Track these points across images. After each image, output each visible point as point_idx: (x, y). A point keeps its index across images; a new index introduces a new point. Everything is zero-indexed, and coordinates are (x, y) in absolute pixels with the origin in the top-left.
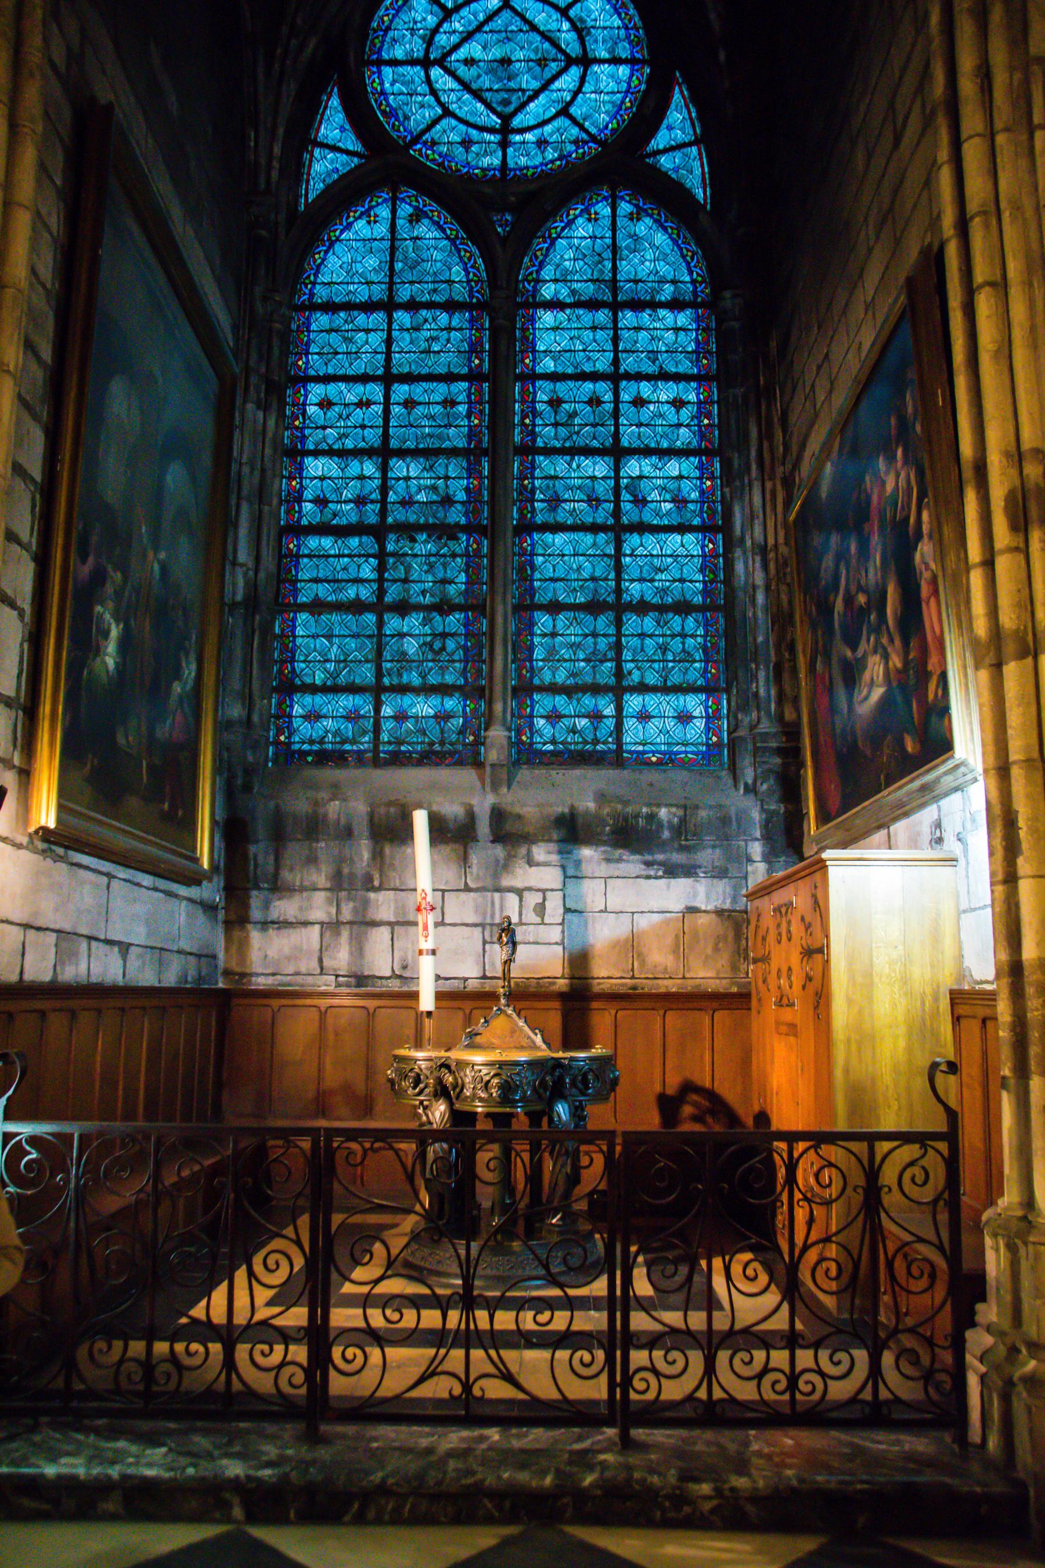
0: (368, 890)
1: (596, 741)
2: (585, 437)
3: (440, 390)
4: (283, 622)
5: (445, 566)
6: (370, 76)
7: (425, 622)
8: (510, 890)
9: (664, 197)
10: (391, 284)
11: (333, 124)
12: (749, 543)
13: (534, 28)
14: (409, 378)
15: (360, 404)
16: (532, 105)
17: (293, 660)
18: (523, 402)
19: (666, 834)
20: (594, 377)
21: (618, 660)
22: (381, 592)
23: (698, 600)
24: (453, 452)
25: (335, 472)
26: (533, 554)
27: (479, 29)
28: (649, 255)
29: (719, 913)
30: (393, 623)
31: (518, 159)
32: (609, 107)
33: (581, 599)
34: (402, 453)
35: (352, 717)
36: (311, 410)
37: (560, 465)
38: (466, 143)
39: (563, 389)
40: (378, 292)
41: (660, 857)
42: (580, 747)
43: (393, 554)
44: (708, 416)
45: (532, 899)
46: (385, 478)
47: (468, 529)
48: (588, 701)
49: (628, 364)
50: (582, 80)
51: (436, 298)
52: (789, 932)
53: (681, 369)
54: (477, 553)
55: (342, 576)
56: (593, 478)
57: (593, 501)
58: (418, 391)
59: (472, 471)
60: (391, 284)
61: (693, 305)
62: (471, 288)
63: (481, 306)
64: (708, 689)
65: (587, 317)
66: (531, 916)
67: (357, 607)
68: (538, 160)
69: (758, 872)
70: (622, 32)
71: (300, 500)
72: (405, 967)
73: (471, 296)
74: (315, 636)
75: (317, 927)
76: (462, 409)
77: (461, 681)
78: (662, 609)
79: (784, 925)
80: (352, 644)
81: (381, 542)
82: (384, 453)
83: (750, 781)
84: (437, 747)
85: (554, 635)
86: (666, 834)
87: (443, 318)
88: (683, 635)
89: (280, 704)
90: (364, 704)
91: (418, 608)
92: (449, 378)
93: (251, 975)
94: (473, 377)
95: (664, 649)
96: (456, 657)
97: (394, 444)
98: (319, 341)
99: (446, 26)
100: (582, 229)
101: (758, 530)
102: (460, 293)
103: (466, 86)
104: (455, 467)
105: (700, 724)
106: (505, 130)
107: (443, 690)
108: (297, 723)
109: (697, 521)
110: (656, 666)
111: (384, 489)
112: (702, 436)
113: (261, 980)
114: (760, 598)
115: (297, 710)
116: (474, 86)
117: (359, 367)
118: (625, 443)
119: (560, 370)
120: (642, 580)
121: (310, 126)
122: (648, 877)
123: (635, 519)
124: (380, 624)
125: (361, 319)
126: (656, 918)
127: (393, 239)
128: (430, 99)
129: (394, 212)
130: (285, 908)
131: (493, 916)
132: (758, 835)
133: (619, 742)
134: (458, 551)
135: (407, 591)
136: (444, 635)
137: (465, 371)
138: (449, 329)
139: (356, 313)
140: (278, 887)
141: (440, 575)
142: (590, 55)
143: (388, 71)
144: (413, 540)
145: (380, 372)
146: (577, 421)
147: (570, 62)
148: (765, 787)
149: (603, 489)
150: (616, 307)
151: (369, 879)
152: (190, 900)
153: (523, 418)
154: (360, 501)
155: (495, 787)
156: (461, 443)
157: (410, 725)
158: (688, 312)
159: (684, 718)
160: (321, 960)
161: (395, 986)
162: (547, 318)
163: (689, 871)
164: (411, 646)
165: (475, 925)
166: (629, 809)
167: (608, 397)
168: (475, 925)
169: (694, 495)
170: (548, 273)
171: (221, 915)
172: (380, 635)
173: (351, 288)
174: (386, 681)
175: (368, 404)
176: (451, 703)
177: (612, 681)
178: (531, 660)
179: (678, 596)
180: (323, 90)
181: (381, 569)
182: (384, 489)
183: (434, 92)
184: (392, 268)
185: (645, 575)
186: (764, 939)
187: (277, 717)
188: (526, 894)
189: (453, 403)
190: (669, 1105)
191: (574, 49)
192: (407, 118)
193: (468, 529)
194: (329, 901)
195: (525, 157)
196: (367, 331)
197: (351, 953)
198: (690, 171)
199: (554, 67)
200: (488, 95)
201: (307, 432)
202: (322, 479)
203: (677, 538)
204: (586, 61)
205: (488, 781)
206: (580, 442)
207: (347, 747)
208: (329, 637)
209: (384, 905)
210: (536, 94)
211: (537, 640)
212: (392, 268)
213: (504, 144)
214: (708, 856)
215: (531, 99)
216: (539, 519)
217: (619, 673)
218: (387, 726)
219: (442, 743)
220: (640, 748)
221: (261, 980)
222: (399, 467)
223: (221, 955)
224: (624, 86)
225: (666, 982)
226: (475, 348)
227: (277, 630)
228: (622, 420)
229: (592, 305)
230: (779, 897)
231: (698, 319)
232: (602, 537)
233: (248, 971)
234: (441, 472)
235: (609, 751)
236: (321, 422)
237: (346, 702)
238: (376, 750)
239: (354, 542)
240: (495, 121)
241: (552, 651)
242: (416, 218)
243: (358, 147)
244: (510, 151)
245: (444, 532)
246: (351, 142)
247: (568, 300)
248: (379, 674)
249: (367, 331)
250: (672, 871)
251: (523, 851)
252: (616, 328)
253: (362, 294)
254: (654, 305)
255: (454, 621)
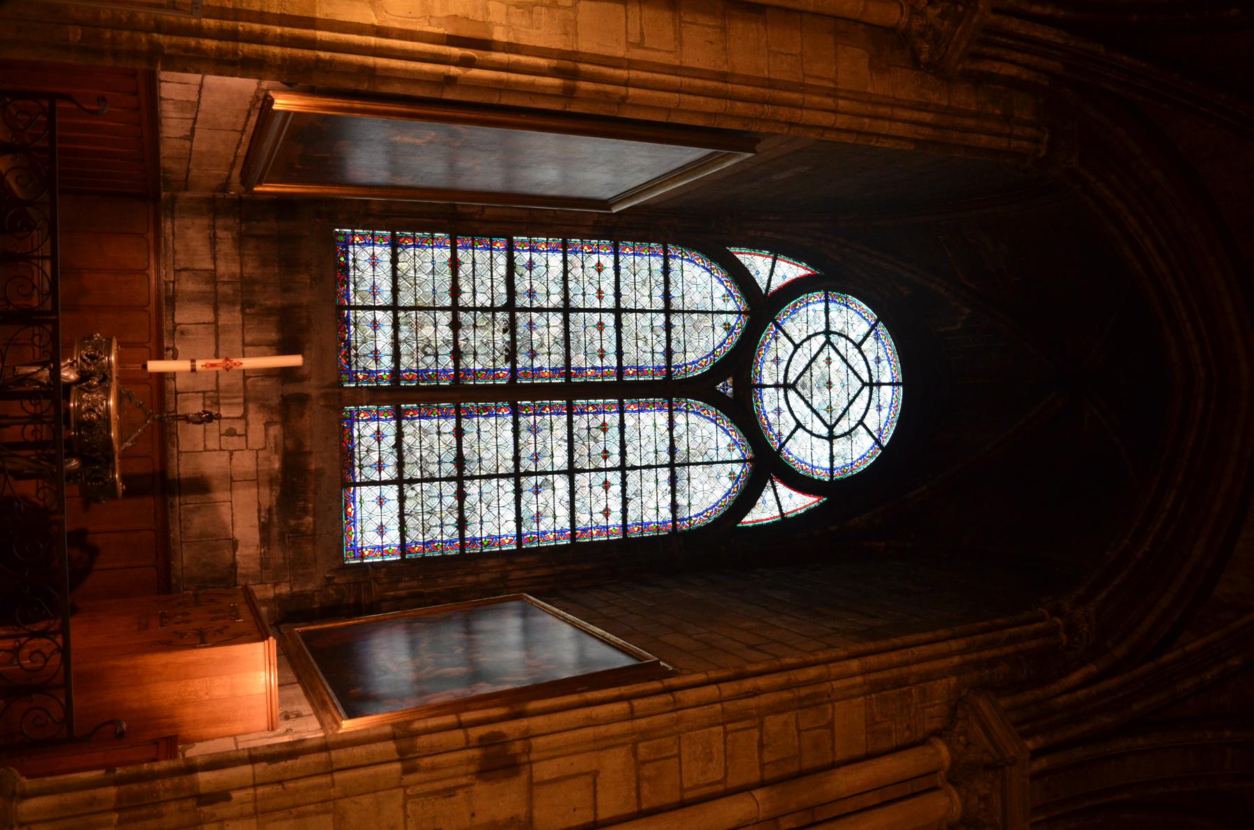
0: (242, 305)
1: (361, 467)
2: (580, 449)
3: (611, 347)
4: (444, 239)
5: (487, 354)
6: (820, 295)
7: (446, 343)
8: (246, 410)
9: (747, 496)
10: (683, 312)
11: (788, 271)
12: (509, 568)
13: (850, 403)
14: (618, 325)
15: (600, 291)
16: (802, 402)
17: (415, 246)
18: (604, 405)
19: (292, 522)
20: (623, 453)
21: (422, 480)
22: (467, 310)
23: (468, 534)
24: (568, 359)
25: (551, 277)
26: (496, 415)
27: (849, 366)
28: (707, 487)
29: (234, 565)
30: (444, 318)
31: (768, 393)
32: (803, 454)
33: (465, 451)
34: (566, 322)
35: (374, 290)
36: (595, 257)
37: (561, 431)
38: (777, 360)
39: (614, 432)
40: (676, 303)
41: (275, 519)
42: (357, 455)
43: (493, 317)
44: (599, 534)
45: (239, 427)
46: (548, 310)
47: (513, 370)
48: (391, 460)
49: (632, 477)
50: (819, 437)
51: (673, 344)
52: (217, 618)
53: (630, 513)
54: (496, 377)
55: (478, 281)
56: (552, 456)
57: (536, 457)
58: (610, 332)
59: (554, 369)
60: (683, 312)
61: (674, 519)
62: (680, 366)
63: (669, 373)
64: (403, 546)
65: (664, 446)
66: (225, 426)
67: (455, 291)
68: (768, 409)
69: (264, 592)
70: (849, 461)
71: (532, 250)
72: (182, 333)
73: (675, 367)
74: (433, 262)
75: (212, 267)
76: (598, 363)
77: (402, 368)
78: (461, 509)
79: (222, 614)
80: (429, 289)
81: (502, 309)
82: (566, 309)
83: (336, 581)
84: (353, 352)
85: (439, 433)
86: (292, 522)
87: (660, 348)
88: (442, 526)
89: (383, 237)
90: (385, 298)
91: (456, 337)
92: (619, 353)
93: (173, 218)
94: (620, 369)
95: (431, 513)
96: (420, 364)
97: (572, 316)
98: (642, 262)
99: (850, 345)
100: (724, 440)
101: (519, 574)
102: (677, 359)
103: (813, 359)
104: (557, 360)
105: (378, 542)
106: (787, 386)
107: (396, 356)
108: (369, 249)
109: (524, 530)
110: (419, 507)
111: (540, 310)
112: (584, 530)
113: (169, 225)
114: (470, 579)
115: (378, 250)
116: (813, 365)
117: (625, 290)
118: (578, 477)
119: (627, 430)
120: (481, 493)
121: (786, 255)
122: (259, 511)
123: (524, 487)
124: (443, 309)
125: (658, 292)
126: (228, 519)
127: (713, 312)
128: (804, 336)
129: (731, 312)
130: (226, 245)
131: (225, 398)
132: (296, 589)
133: (362, 484)
134: (497, 364)
135: (468, 327)
136: (436, 355)
137: (625, 364)
138: (653, 352)
139: (662, 287)
140: (241, 241)
141: (479, 351)
142: (835, 441)
143: (822, 306)
144: (505, 331)
145: (623, 306)
146: (592, 443)
147: (831, 428)
148: (331, 592)
149: (544, 464)
150: (672, 466)
151: (251, 305)
152: (229, 177)
153: (593, 405)
154: (531, 293)
155: (325, 396)
156: (574, 363)
157: (370, 332)
158: (670, 516)
159: (381, 530)
160: (186, 269)
161: (167, 325)
162: (662, 418)
163: (265, 540)
164: (427, 331)
165: (217, 385)
166: (311, 494)
167: (609, 465)
168: (217, 385)
169: (542, 528)
170: (693, 418)
171: (220, 195)
172: (435, 309)
173: (680, 285)
174: (401, 314)
175: (600, 298)
176: (386, 362)
177: (406, 477)
178: (420, 418)
179: (470, 520)
180: (809, 264)
181: (484, 309)
182: (540, 310)
183: (809, 338)
184: (693, 312)
185: (484, 496)
186: (212, 601)
187: (373, 235)
188: (243, 422)
189: (602, 357)
190: (79, 537)
191: (838, 430)
192: (792, 320)
193: (513, 370)
194: (233, 275)
195: (770, 400)
196: (650, 296)
197: (192, 292)
198: (764, 511)
199: (826, 417)
200: (808, 374)
201: (580, 255)
202: (547, 266)
203: (512, 516)
204: (831, 438)
205: (329, 390)
206: (577, 446)
207: (352, 287)
208: (433, 272)
209: (231, 317)
210: (810, 406)
211: (435, 421)
212: (693, 312)
213: (777, 386)
214: (277, 555)
215: (806, 402)
216: (521, 419)
217: (412, 481)
218: (369, 315)
219: (356, 356)
220: (358, 499)
221: (169, 225)
222: (556, 319)
223: (188, 194)
224: (815, 464)
225: (177, 529)
226: (639, 370)
227: (437, 235)
228: (593, 474)
229: (672, 450)
230: (244, 610)
231: (665, 523)
232: (511, 464)
233: (176, 215)
234: (553, 350)
235: (354, 477)
236: (586, 265)
237: (386, 286)
238: (350, 308)
239: (502, 289)
240: (792, 378)
241: (427, 433)
242: (728, 328)
243: (774, 287)
244: (773, 390)
245: (511, 355)
246: (777, 283)
247: (675, 433)
248: (405, 309)
249: (650, 296)
250: (264, 528)
251: (276, 418)
252: (656, 467)
253: (675, 292)
254: (673, 492)
255: (447, 362)
